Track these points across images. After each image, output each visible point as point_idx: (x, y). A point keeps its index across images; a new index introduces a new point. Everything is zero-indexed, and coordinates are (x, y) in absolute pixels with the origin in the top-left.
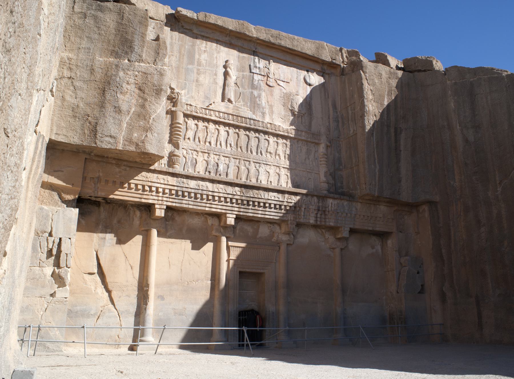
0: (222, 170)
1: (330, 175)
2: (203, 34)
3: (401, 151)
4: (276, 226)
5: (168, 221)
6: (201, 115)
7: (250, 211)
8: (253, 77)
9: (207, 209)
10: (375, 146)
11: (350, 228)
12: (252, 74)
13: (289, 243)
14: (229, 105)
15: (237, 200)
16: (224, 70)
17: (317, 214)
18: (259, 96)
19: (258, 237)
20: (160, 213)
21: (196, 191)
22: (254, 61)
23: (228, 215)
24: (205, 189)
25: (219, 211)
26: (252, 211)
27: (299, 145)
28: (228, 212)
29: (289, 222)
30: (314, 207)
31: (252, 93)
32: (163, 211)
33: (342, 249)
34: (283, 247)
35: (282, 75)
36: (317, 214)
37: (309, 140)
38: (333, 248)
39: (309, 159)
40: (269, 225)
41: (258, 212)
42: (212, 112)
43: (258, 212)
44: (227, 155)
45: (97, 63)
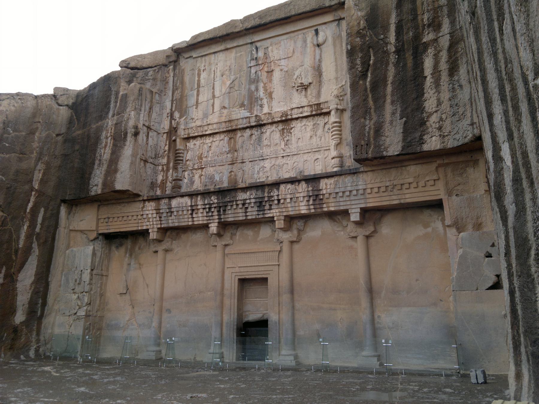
0: (218, 179)
1: (347, 145)
2: (201, 55)
3: (426, 77)
5: (175, 240)
6: (196, 134)
7: (230, 216)
8: (250, 72)
9: (190, 223)
10: (369, 90)
11: (361, 208)
12: (249, 69)
13: (291, 240)
14: (223, 113)
15: (215, 207)
16: (221, 78)
17: (308, 201)
18: (257, 89)
19: (258, 239)
20: (153, 235)
21: (178, 209)
22: (252, 54)
23: (210, 225)
24: (184, 205)
25: (201, 222)
26: (233, 215)
27: (303, 124)
28: (209, 222)
29: (275, 219)
30: (302, 195)
31: (249, 89)
32: (155, 233)
33: (368, 237)
34: (286, 247)
35: (281, 53)
36: (308, 201)
37: (314, 113)
38: (356, 237)
39: (316, 135)
41: (239, 215)
42: (206, 128)
43: (239, 215)
44: (222, 164)
45: (92, 130)
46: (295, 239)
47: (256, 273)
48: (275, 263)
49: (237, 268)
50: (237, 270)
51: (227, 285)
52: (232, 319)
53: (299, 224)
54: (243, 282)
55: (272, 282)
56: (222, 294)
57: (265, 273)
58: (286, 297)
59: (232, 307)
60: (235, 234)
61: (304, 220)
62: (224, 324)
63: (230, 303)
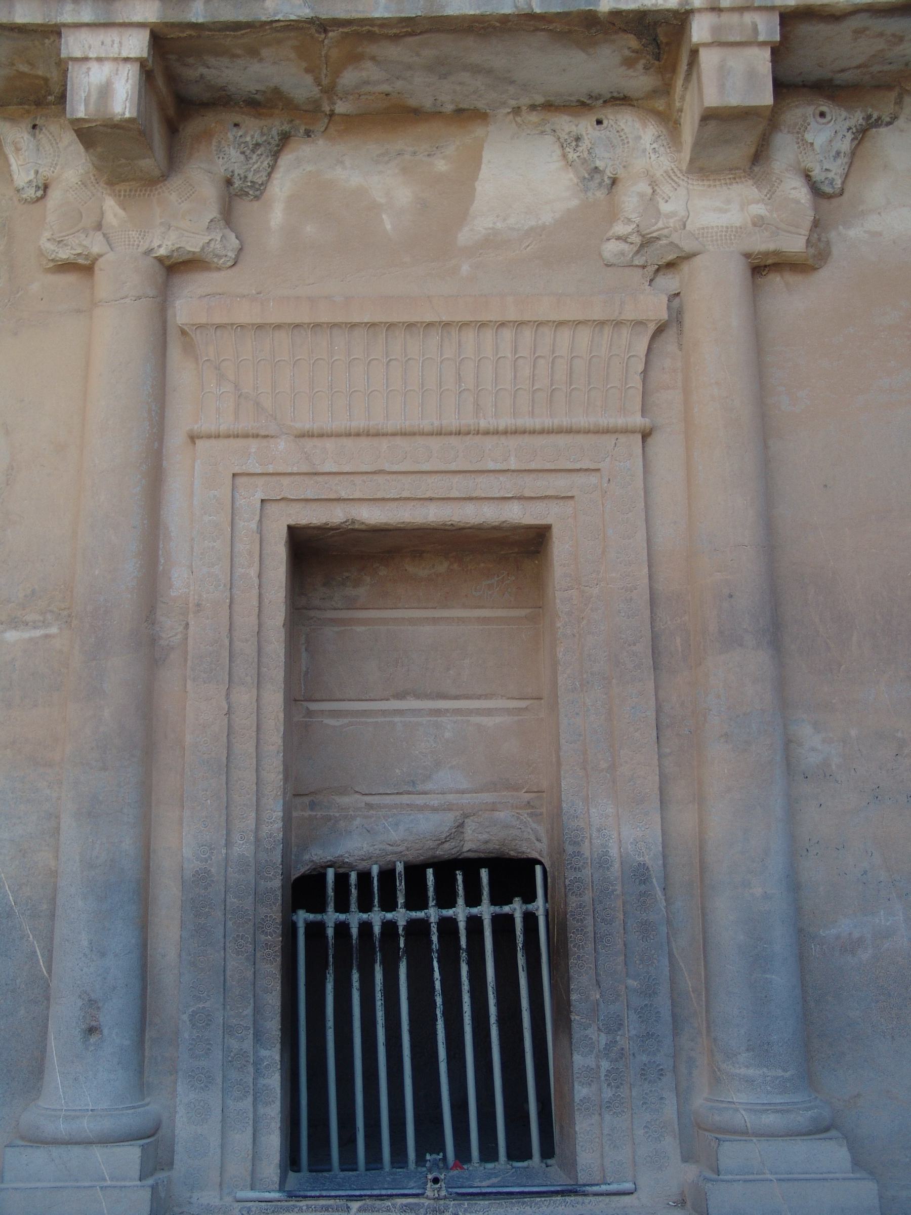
4: (626, 122)
13: (762, 243)
19: (464, 237)
23: (74, 45)
29: (700, 30)
34: (715, 293)
40: (566, 124)
46: (794, 244)
47: (458, 486)
48: (620, 421)
49: (282, 445)
50: (283, 453)
51: (190, 575)
52: (243, 848)
53: (822, 134)
54: (319, 558)
55: (589, 562)
56: (150, 650)
57: (532, 485)
58: (732, 678)
59: (245, 746)
60: (258, 191)
61: (858, 118)
62: (169, 896)
63: (226, 714)
